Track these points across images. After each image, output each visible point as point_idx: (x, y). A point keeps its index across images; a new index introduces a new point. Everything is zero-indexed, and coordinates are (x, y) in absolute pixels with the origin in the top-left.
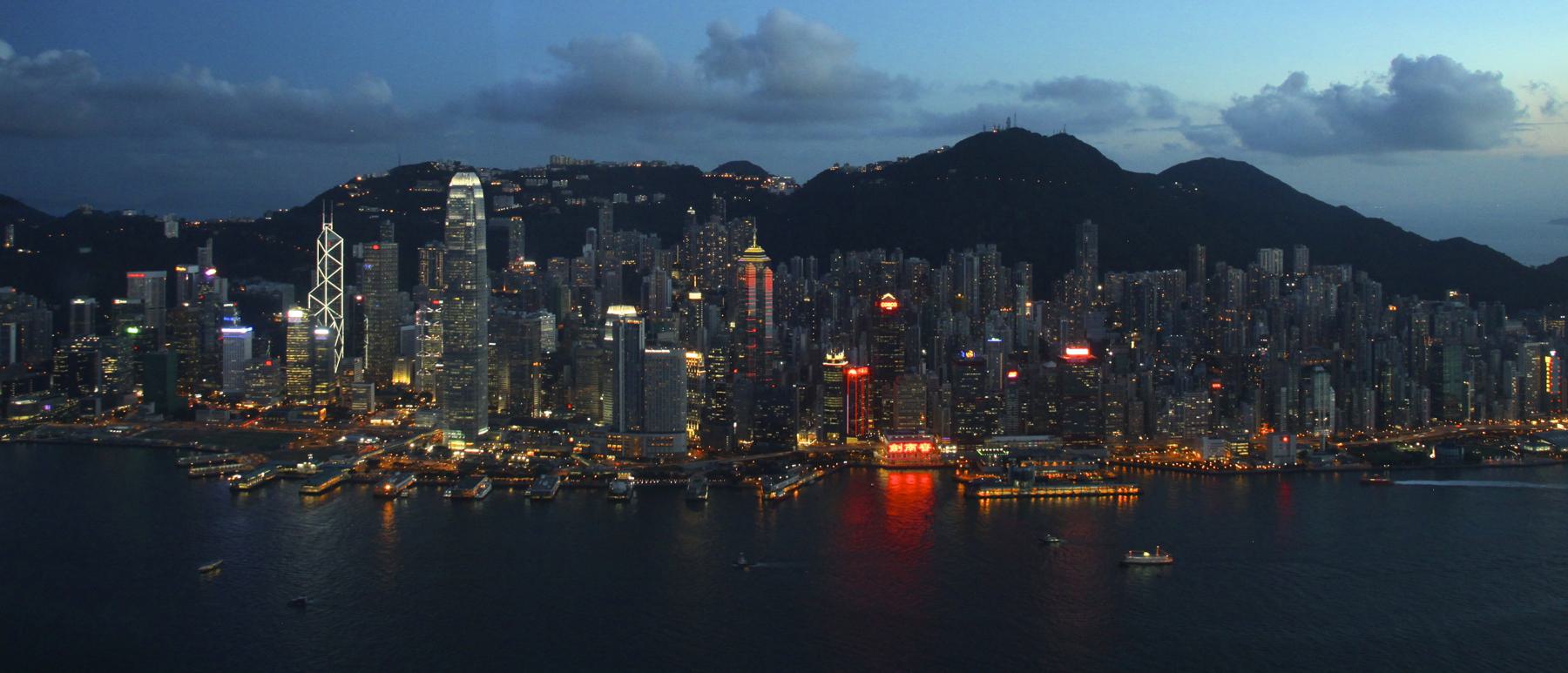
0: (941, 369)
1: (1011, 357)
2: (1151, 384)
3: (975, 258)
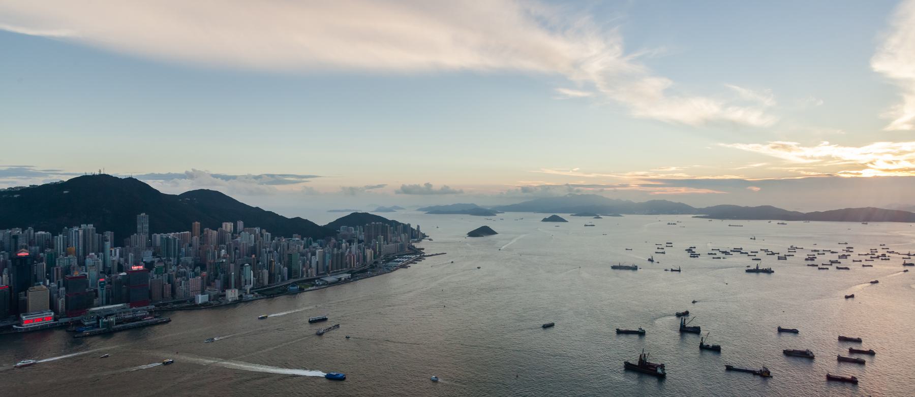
0: (59, 282)
1: (101, 272)
2: (174, 276)
3: (80, 231)
